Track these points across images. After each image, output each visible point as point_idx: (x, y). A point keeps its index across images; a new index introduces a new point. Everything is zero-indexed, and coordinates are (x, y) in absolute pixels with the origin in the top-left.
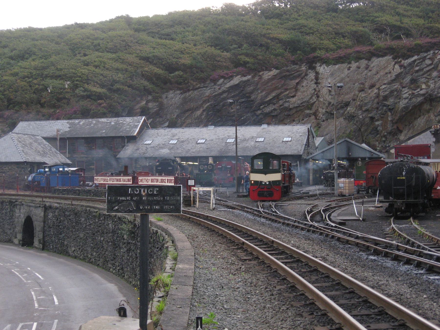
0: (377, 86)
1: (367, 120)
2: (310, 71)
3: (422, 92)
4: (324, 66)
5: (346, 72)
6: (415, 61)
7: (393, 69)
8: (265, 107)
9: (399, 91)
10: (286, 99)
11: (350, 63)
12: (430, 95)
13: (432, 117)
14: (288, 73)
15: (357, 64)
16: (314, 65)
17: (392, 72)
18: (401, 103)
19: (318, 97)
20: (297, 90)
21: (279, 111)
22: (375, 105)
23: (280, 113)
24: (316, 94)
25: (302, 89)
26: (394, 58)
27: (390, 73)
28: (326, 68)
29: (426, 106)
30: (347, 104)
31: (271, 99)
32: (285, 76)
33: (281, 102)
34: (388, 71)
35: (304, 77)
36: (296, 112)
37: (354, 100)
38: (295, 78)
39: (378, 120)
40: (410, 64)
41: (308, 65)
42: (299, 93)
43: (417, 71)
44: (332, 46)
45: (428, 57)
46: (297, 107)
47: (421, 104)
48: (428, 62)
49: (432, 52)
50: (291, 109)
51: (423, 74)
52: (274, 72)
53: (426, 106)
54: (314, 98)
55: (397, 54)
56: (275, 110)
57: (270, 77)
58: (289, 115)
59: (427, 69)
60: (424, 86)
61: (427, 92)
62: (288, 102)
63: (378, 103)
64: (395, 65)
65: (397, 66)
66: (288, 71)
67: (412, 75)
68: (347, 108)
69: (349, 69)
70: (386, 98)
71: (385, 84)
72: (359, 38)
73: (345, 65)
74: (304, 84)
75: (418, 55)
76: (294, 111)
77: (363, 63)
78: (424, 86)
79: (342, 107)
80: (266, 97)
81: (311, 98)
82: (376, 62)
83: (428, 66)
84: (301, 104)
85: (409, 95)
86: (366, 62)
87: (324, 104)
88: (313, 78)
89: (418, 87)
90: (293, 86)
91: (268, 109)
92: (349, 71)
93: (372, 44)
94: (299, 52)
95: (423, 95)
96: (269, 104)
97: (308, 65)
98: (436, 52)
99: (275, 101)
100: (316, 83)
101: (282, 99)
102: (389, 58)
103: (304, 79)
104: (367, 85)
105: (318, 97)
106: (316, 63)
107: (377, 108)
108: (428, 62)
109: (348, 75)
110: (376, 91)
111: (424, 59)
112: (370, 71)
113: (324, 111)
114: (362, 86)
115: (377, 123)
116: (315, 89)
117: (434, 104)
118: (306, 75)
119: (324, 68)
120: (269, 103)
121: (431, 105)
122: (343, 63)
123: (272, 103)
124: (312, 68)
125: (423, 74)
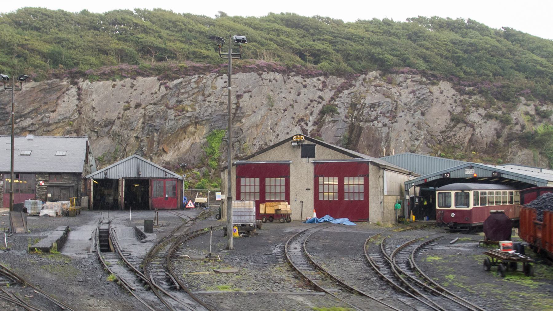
0: (143, 106)
1: (133, 140)
2: (72, 86)
3: (188, 114)
4: (87, 81)
6: (181, 82)
7: (159, 90)
9: (165, 112)
15: (122, 82)
16: (76, 80)
17: (158, 92)
18: (167, 124)
19: (80, 113)
20: (57, 105)
21: (37, 126)
23: (38, 129)
24: (79, 111)
25: (63, 105)
27: (156, 93)
28: (89, 83)
29: (191, 129)
31: (29, 113)
33: (40, 117)
34: (153, 92)
35: (65, 92)
36: (57, 128)
37: (119, 118)
40: (176, 86)
42: (59, 109)
43: (183, 93)
44: (97, 62)
46: (57, 123)
47: (187, 126)
49: (197, 76)
53: (191, 129)
54: (76, 115)
56: (32, 124)
57: (28, 89)
58: (48, 131)
59: (193, 92)
61: (193, 115)
63: (143, 123)
65: (163, 88)
67: (178, 96)
68: (112, 127)
69: (114, 86)
71: (151, 104)
72: (122, 56)
73: (110, 83)
74: (65, 100)
76: (55, 126)
77: (128, 81)
78: (189, 109)
79: (106, 126)
81: (73, 114)
84: (62, 119)
85: (175, 116)
86: (132, 81)
88: (76, 93)
89: (183, 110)
91: (27, 122)
93: (137, 63)
94: (61, 66)
95: (190, 117)
96: (26, 118)
97: (70, 80)
98: (201, 76)
99: (33, 115)
100: (78, 99)
101: (41, 114)
103: (65, 94)
104: (133, 104)
106: (78, 79)
110: (142, 111)
112: (135, 90)
114: (127, 104)
116: (77, 105)
117: (199, 126)
118: (68, 90)
119: (87, 84)
120: (25, 116)
121: (196, 128)
122: (108, 79)
124: (76, 84)
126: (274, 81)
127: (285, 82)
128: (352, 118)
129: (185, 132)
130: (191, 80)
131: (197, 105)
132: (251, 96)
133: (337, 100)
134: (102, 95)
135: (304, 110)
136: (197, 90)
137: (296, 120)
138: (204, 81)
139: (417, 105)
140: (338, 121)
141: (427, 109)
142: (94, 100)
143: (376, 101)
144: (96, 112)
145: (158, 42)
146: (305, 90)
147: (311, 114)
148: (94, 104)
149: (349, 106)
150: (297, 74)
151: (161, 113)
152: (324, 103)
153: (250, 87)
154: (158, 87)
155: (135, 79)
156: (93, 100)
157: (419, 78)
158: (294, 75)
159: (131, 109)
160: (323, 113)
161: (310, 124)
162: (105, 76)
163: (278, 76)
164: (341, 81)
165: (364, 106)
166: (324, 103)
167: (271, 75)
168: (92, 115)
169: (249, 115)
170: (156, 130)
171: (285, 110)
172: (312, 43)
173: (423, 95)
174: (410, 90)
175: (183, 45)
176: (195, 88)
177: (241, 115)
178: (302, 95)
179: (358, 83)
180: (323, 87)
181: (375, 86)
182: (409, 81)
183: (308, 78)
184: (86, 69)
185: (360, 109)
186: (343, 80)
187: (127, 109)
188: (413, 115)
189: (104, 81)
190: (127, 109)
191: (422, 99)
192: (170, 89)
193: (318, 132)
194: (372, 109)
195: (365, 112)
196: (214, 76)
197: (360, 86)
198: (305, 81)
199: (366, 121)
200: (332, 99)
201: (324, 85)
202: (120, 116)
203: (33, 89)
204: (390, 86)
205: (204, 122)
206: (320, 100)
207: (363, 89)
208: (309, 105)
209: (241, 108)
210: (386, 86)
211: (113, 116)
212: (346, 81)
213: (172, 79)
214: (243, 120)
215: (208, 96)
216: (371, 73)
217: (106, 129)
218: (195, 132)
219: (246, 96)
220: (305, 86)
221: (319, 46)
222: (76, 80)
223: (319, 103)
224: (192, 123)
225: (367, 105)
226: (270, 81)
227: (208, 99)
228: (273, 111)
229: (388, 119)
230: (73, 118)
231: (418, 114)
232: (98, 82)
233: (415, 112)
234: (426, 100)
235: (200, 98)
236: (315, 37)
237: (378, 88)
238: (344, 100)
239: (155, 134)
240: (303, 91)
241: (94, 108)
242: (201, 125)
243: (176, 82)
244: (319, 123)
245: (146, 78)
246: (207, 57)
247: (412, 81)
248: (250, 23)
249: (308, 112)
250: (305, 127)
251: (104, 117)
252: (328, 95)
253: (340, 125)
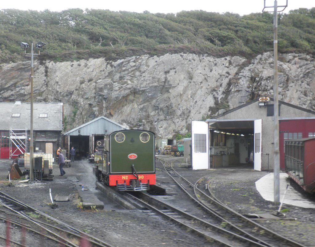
0: (94, 80)
1: (87, 106)
2: (41, 66)
3: (128, 86)
4: (52, 62)
5: (70, 67)
6: (123, 62)
7: (106, 68)
8: (4, 92)
9: (111, 85)
10: (21, 87)
12: (135, 89)
13: (136, 106)
14: (23, 67)
15: (78, 62)
18: (113, 94)
22: (93, 95)
26: (106, 60)
27: (104, 71)
28: (54, 64)
29: (131, 97)
30: (71, 93)
31: (9, 86)
32: (21, 69)
33: (18, 89)
34: (102, 70)
37: (76, 90)
38: (28, 71)
39: (95, 107)
40: (119, 65)
41: (39, 61)
43: (124, 71)
45: (132, 61)
47: (128, 95)
49: (134, 57)
50: (25, 95)
51: (128, 73)
53: (131, 97)
55: (109, 57)
56: (12, 95)
57: (9, 68)
60: (129, 82)
61: (132, 87)
62: (24, 89)
63: (95, 93)
64: (107, 65)
65: (109, 66)
66: (24, 65)
68: (71, 96)
69: (72, 66)
70: (101, 89)
71: (100, 79)
73: (69, 63)
75: (124, 58)
77: (83, 62)
78: (129, 82)
79: (67, 95)
80: (6, 84)
81: (42, 87)
82: (93, 62)
83: (132, 67)
86: (85, 61)
87: (53, 92)
88: (44, 71)
90: (27, 77)
92: (72, 68)
95: (130, 88)
96: (7, 90)
98: (138, 57)
99: (12, 88)
101: (18, 87)
103: (36, 72)
105: (47, 85)
106: (45, 60)
107: (95, 97)
108: (132, 64)
109: (72, 71)
110: (94, 84)
111: (129, 62)
113: (53, 98)
115: (94, 109)
116: (45, 81)
117: (137, 96)
118: (38, 69)
119: (52, 64)
120: (7, 89)
121: (134, 97)
123: (10, 90)
125: (128, 73)
126: (193, 61)
127: (200, 61)
128: (252, 88)
129: (126, 100)
130: (130, 60)
131: (135, 79)
132: (176, 72)
133: (240, 74)
134: (64, 72)
135: (215, 82)
136: (134, 68)
137: (210, 90)
138: (140, 61)
139: (304, 77)
140: (241, 90)
141: (311, 80)
142: (58, 76)
143: (271, 75)
144: (59, 85)
145: (103, 32)
146: (216, 67)
147: (221, 85)
148: (57, 79)
149: (249, 79)
150: (209, 55)
151: (109, 86)
152: (230, 77)
153: (175, 65)
154: (105, 66)
155: (88, 60)
156: (57, 77)
157: (304, 56)
158: (207, 56)
159: (85, 82)
160: (229, 84)
161: (220, 93)
162: (65, 58)
163: (195, 56)
164: (243, 60)
165: (261, 79)
166: (230, 77)
167: (191, 56)
168: (57, 88)
169: (175, 87)
170: (104, 98)
171: (201, 83)
172: (219, 31)
173: (308, 69)
174: (298, 66)
175: (123, 35)
176: (135, 66)
177: (169, 86)
178: (214, 71)
179: (256, 61)
180: (229, 65)
181: (270, 63)
182: (296, 59)
183: (218, 58)
184: (51, 52)
185: (259, 81)
186: (245, 60)
187: (82, 83)
188: (301, 85)
189: (65, 62)
190: (82, 83)
191: (307, 73)
192: (115, 67)
193: (225, 99)
194: (268, 81)
195: (263, 83)
196: (147, 57)
197: (257, 64)
198: (215, 60)
199: (264, 91)
200: (237, 74)
201: (230, 63)
202: (78, 88)
203: (12, 68)
204: (282, 63)
205: (141, 92)
206: (227, 75)
207: (260, 67)
208: (219, 79)
209: (169, 81)
210: (279, 63)
211: (73, 88)
212: (246, 60)
213: (115, 60)
214: (170, 91)
215: (144, 72)
216: (266, 53)
217: (66, 98)
218: (134, 100)
219: (172, 72)
220: (216, 65)
221: (224, 33)
222: (44, 62)
223: (227, 77)
224: (132, 93)
225: (264, 78)
226: (190, 61)
227: (144, 75)
228: (192, 83)
229: (282, 89)
230: (42, 90)
231: (304, 85)
232: (60, 63)
233: (302, 82)
234: (311, 73)
235: (137, 73)
236: (221, 27)
237: (272, 65)
238: (245, 75)
239: (104, 102)
240: (214, 68)
241: (57, 82)
242: (138, 94)
243: (119, 61)
244: (227, 92)
245: (96, 60)
246: (141, 43)
247: (299, 59)
248: (170, 17)
249: (218, 84)
250: (216, 96)
251: (66, 89)
252: (233, 70)
253: (243, 93)
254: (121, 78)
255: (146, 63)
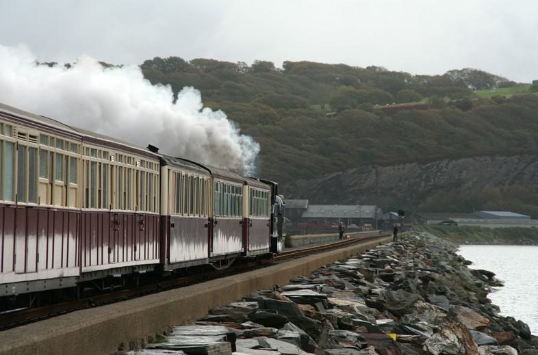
3: (432, 183)
11: (394, 166)
30: (392, 189)
40: (426, 168)
48: (435, 167)
52: (354, 170)
54: (375, 185)
77: (401, 166)
78: (432, 181)
82: (408, 165)
91: (351, 190)
102: (415, 164)
124: (374, 168)
163: (489, 158)
200: (523, 169)
213: (424, 164)
219: (464, 172)
220: (505, 163)
235: (439, 174)
254: (428, 177)
255: (447, 165)
